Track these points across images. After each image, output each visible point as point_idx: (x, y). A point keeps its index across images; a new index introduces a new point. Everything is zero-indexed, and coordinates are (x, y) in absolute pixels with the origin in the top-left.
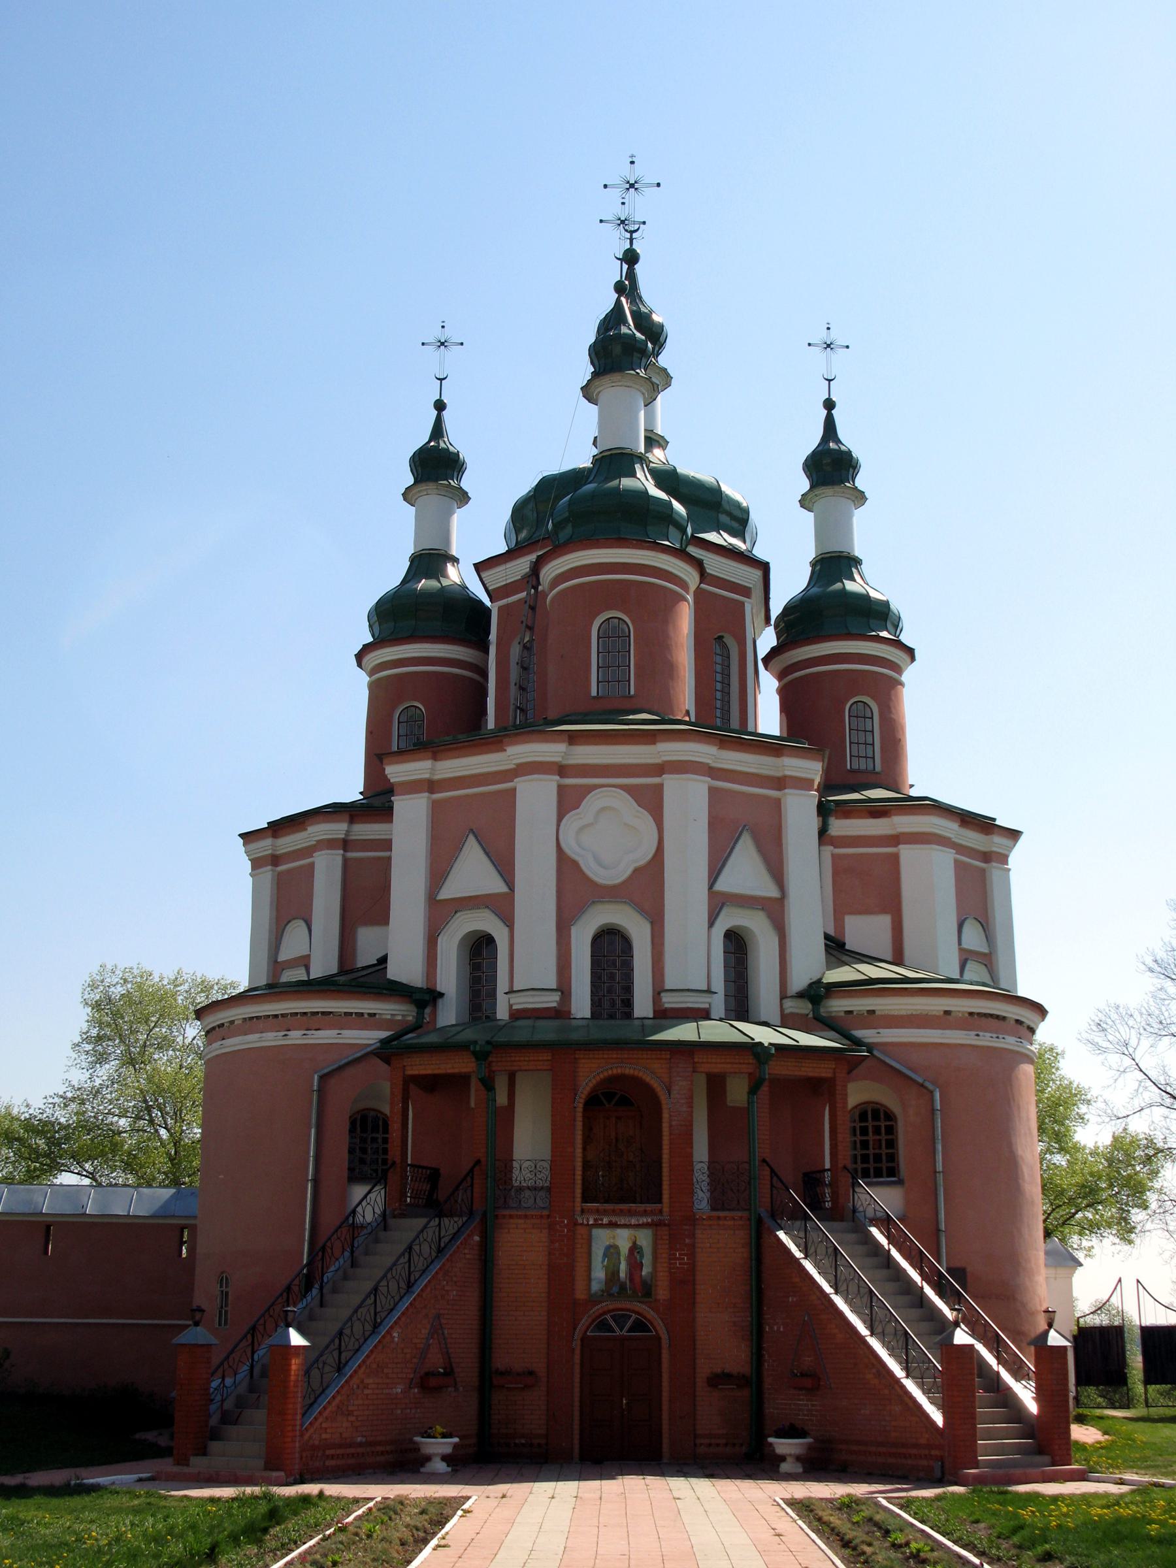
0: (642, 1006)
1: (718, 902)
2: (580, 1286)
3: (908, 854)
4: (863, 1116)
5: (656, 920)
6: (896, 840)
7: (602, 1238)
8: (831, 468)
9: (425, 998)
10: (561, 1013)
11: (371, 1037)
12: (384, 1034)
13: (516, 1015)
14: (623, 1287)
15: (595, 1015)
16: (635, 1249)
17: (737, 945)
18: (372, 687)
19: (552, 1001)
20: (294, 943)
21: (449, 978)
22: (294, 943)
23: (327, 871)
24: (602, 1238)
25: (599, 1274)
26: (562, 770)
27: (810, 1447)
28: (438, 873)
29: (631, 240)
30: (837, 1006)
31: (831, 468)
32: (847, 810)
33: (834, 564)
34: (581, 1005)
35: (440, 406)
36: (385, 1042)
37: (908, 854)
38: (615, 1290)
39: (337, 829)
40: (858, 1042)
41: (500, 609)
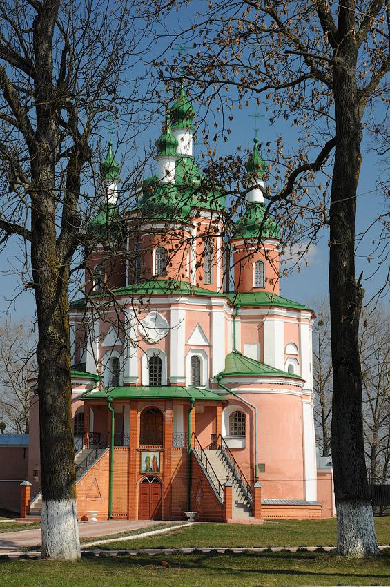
0: (164, 381)
2: (138, 468)
4: (236, 416)
15: (151, 384)
16: (154, 458)
17: (196, 361)
24: (145, 455)
25: (144, 465)
27: (196, 515)
32: (245, 307)
34: (146, 380)
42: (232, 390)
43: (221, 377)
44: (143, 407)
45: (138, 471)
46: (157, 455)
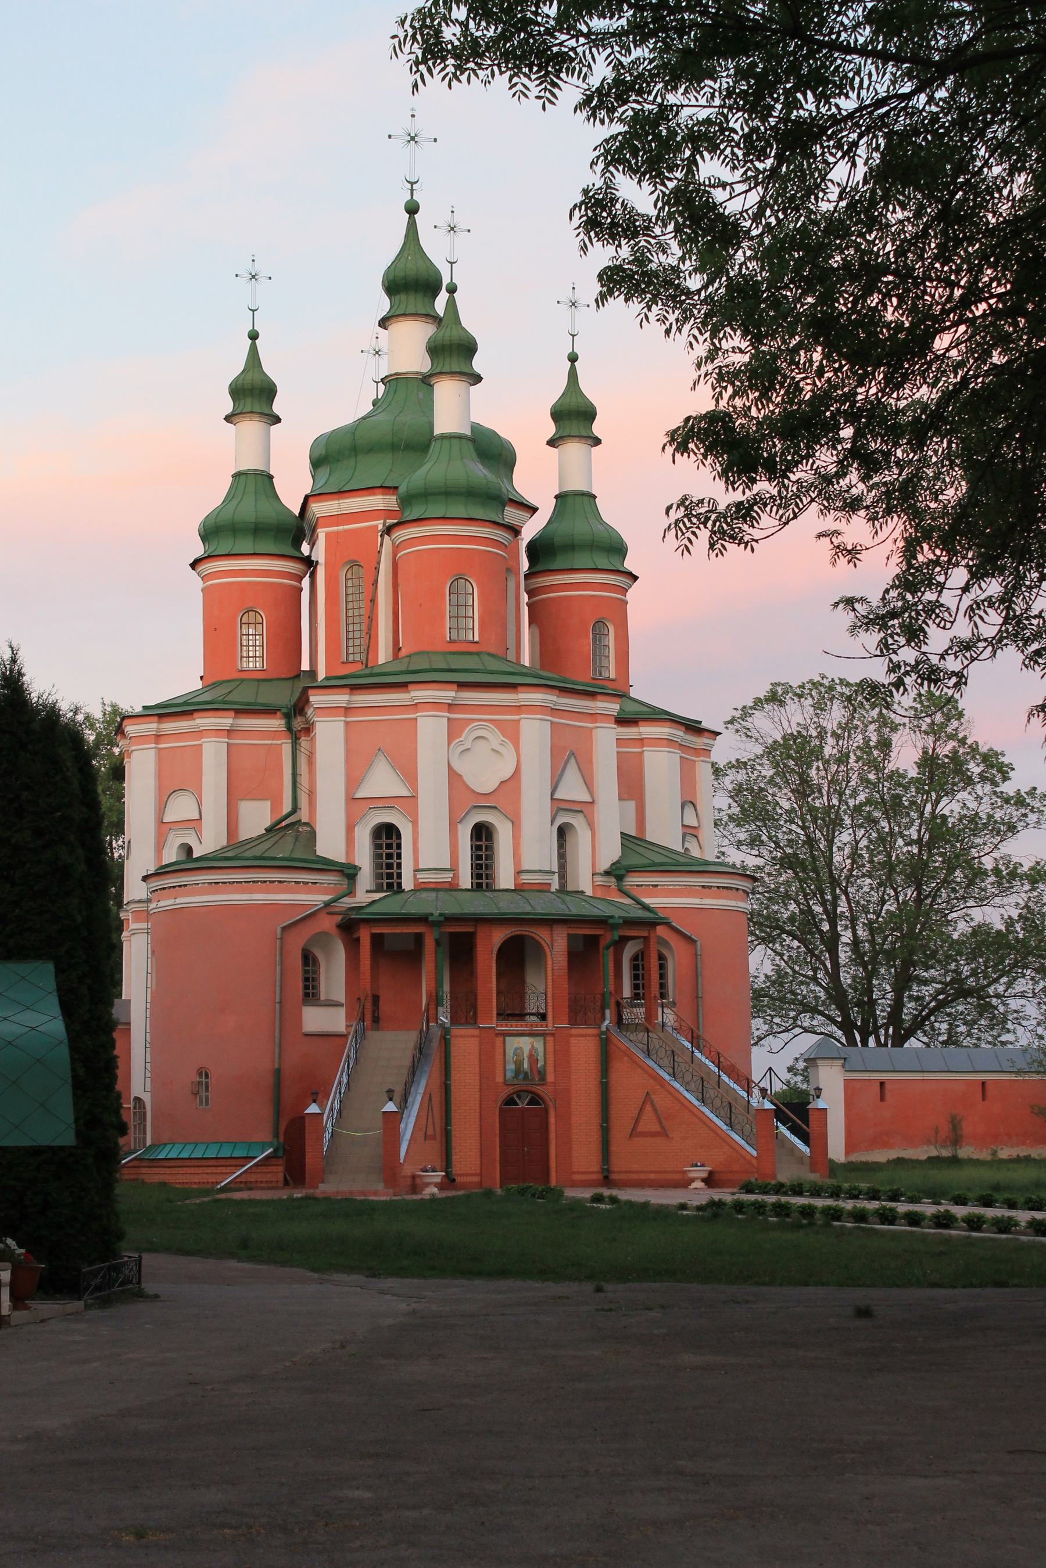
1: (559, 806)
6: (641, 741)
9: (349, 872)
11: (318, 899)
12: (327, 898)
14: (526, 1074)
19: (447, 877)
20: (181, 808)
21: (364, 858)
22: (181, 808)
23: (213, 755)
28: (353, 780)
29: (412, 190)
30: (633, 880)
31: (574, 418)
33: (574, 502)
34: (466, 881)
35: (254, 336)
36: (327, 904)
38: (521, 1076)
39: (226, 721)
40: (646, 907)
41: (327, 535)
42: (647, 901)
43: (622, 872)
44: (499, 936)
45: (500, 1079)
46: (539, 1044)
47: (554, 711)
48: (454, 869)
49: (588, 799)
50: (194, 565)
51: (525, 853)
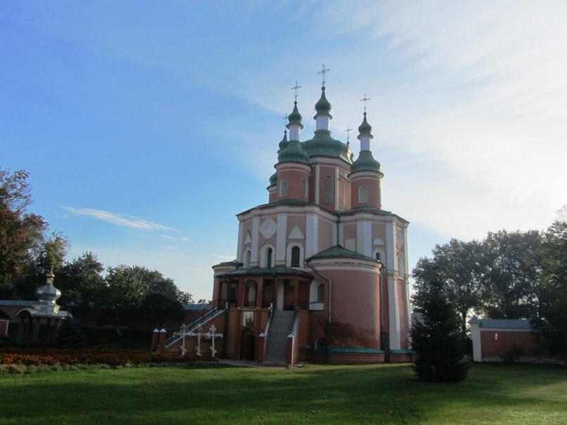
1: (288, 241)
3: (358, 223)
5: (275, 247)
7: (245, 313)
8: (365, 130)
10: (258, 267)
13: (276, 266)
17: (296, 251)
18: (270, 195)
19: (255, 265)
26: (260, 215)
30: (313, 262)
31: (365, 130)
33: (365, 153)
37: (358, 223)
40: (315, 270)
47: (288, 212)
48: (259, 262)
49: (302, 237)
50: (267, 189)
51: (282, 257)
